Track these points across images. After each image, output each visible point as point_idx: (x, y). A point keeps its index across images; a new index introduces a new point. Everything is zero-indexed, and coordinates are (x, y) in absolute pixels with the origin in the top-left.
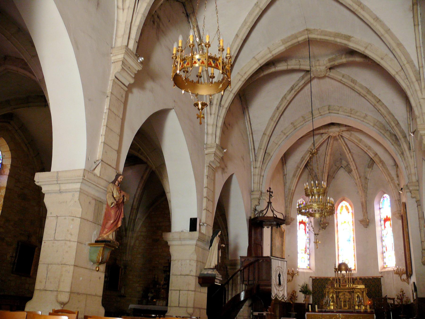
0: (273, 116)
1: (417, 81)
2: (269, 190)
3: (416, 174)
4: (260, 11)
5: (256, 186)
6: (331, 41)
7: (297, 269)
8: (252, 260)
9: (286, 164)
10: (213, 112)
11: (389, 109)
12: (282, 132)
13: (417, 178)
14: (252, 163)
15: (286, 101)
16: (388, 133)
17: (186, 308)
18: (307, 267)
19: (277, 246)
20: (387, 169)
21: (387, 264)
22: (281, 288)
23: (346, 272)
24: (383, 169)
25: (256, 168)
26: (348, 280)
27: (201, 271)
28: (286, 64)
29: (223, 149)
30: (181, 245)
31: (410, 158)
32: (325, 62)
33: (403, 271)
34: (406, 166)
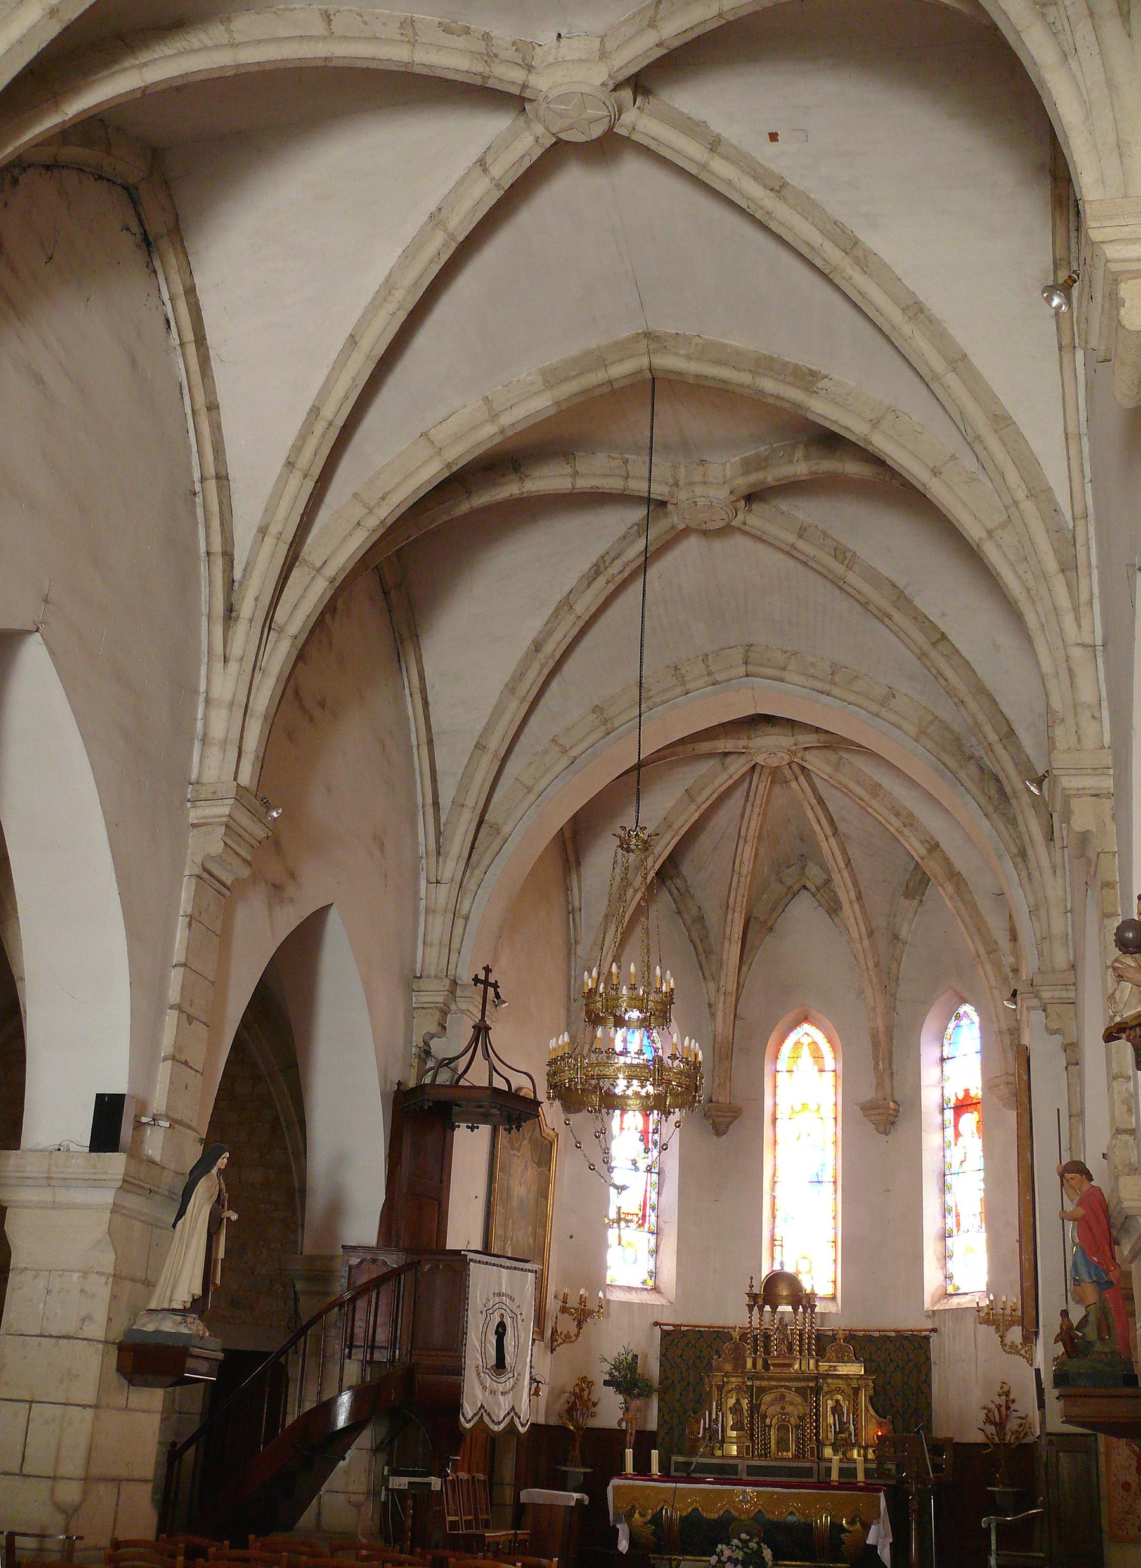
0: (519, 675)
1: (1063, 571)
2: (482, 977)
3: (1070, 937)
4: (445, 245)
5: (433, 954)
6: (742, 385)
7: (601, 1294)
8: (393, 1260)
9: (582, 870)
10: (236, 649)
11: (979, 672)
12: (554, 740)
13: (1071, 957)
14: (424, 861)
15: (572, 618)
16: (973, 769)
17: (49, 1482)
18: (644, 1282)
19: (515, 1202)
20: (973, 907)
21: (956, 1281)
22: (505, 1383)
23: (795, 1309)
24: (960, 904)
25: (438, 882)
26: (801, 1341)
27: (135, 1316)
28: (568, 470)
29: (268, 806)
30: (55, 1206)
31: (1048, 872)
32: (728, 473)
33: (1011, 1315)
34: (1032, 901)
